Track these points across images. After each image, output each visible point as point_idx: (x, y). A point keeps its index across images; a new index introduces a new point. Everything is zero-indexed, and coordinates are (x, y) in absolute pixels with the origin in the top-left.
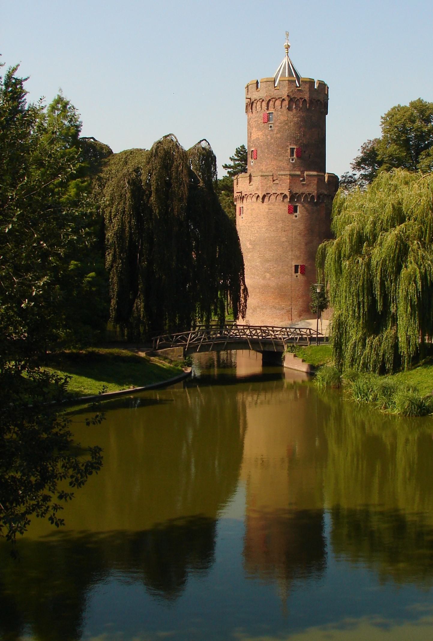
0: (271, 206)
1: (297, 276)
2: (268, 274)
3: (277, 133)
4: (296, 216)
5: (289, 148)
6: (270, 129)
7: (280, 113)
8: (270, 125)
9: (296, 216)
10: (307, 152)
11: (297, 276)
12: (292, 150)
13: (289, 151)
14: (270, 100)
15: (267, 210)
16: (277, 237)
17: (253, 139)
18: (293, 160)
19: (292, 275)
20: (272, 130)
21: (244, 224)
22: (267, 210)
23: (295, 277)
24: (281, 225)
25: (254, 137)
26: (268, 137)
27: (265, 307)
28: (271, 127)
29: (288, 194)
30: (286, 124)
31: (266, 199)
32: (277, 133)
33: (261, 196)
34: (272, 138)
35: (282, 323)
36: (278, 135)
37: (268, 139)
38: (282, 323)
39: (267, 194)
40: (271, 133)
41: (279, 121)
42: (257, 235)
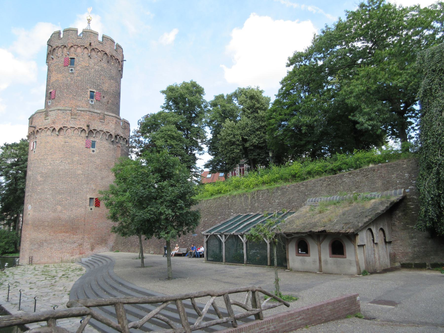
0: (68, 140)
1: (91, 209)
2: (59, 207)
3: (77, 76)
4: (93, 151)
6: (70, 72)
7: (81, 59)
8: (70, 69)
9: (93, 151)
10: (105, 98)
11: (91, 209)
13: (89, 93)
14: (72, 46)
15: (63, 143)
16: (72, 169)
17: (51, 82)
19: (86, 207)
20: (73, 73)
21: (36, 158)
22: (63, 143)
23: (90, 210)
25: (53, 79)
26: (68, 79)
27: (53, 241)
29: (86, 128)
30: (87, 69)
31: (62, 133)
32: (77, 76)
33: (57, 129)
34: (72, 80)
35: (72, 258)
36: (79, 78)
37: (68, 80)
38: (72, 258)
40: (72, 75)
41: (80, 65)
42: (50, 167)
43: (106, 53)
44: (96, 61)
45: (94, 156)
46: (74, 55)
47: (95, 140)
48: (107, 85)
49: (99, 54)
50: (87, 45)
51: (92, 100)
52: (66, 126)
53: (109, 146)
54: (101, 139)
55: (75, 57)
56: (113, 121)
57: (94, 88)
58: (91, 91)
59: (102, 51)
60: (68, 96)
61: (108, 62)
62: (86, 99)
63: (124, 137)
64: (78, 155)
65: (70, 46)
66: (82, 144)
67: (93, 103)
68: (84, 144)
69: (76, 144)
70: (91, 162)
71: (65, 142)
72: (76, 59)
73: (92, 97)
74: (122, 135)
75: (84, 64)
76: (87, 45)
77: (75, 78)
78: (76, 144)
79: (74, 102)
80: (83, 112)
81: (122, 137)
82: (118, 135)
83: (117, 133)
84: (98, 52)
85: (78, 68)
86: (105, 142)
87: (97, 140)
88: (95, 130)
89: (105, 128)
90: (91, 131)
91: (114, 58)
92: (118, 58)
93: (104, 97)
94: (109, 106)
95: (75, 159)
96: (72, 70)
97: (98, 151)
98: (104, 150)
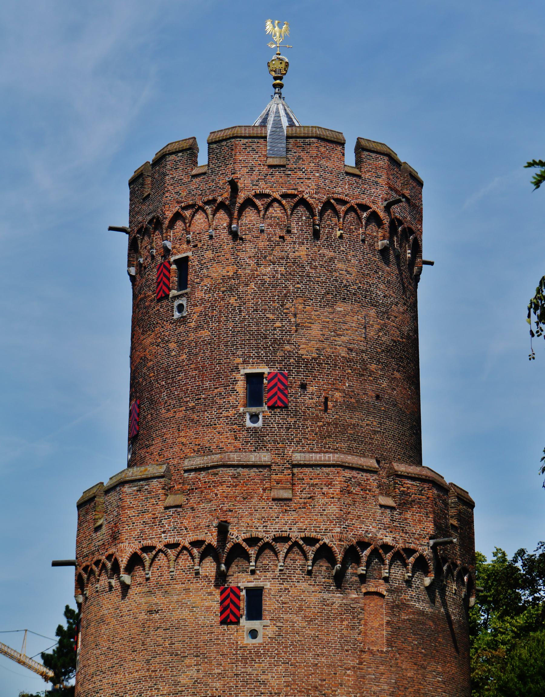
0: (158, 600)
3: (198, 327)
4: (253, 634)
5: (240, 377)
6: (177, 315)
7: (209, 254)
8: (176, 303)
9: (253, 634)
10: (310, 389)
12: (253, 380)
13: (241, 386)
15: (143, 616)
18: (254, 417)
22: (143, 616)
24: (192, 672)
26: (172, 345)
28: (180, 308)
32: (198, 327)
36: (205, 334)
39: (147, 549)
41: (207, 281)
43: (303, 202)
44: (261, 245)
45: (256, 655)
46: (185, 246)
47: (260, 584)
48: (316, 330)
49: (276, 211)
50: (224, 195)
51: (254, 410)
52: (148, 542)
53: (324, 601)
54: (283, 576)
55: (189, 254)
56: (330, 484)
57: (260, 360)
58: (248, 376)
59: (285, 196)
60: (171, 414)
61: (316, 235)
62: (232, 412)
63: (400, 545)
64: (193, 661)
65: (169, 215)
66: (208, 608)
67: (260, 424)
68: (216, 607)
69: (186, 613)
70: (246, 683)
71: (150, 612)
72: (194, 263)
73: (254, 396)
74: (388, 540)
75: (217, 271)
76: (224, 195)
77: (192, 336)
78: (186, 613)
79: (191, 433)
80: (203, 474)
81: (387, 548)
82: (364, 545)
83: (351, 537)
84: (269, 205)
85: (199, 294)
86: (304, 585)
87: (267, 582)
88: (252, 541)
89: (295, 525)
90: (237, 546)
91: (342, 209)
92: (366, 201)
93: (303, 387)
94: (328, 418)
95: (184, 680)
96: (180, 308)
97: (271, 631)
98: (299, 621)
